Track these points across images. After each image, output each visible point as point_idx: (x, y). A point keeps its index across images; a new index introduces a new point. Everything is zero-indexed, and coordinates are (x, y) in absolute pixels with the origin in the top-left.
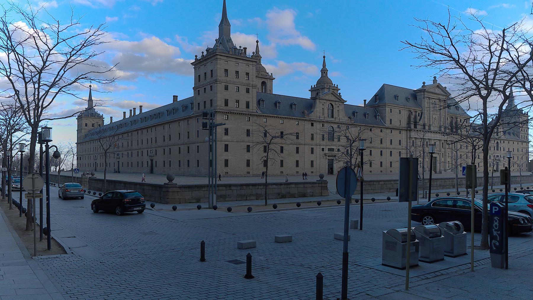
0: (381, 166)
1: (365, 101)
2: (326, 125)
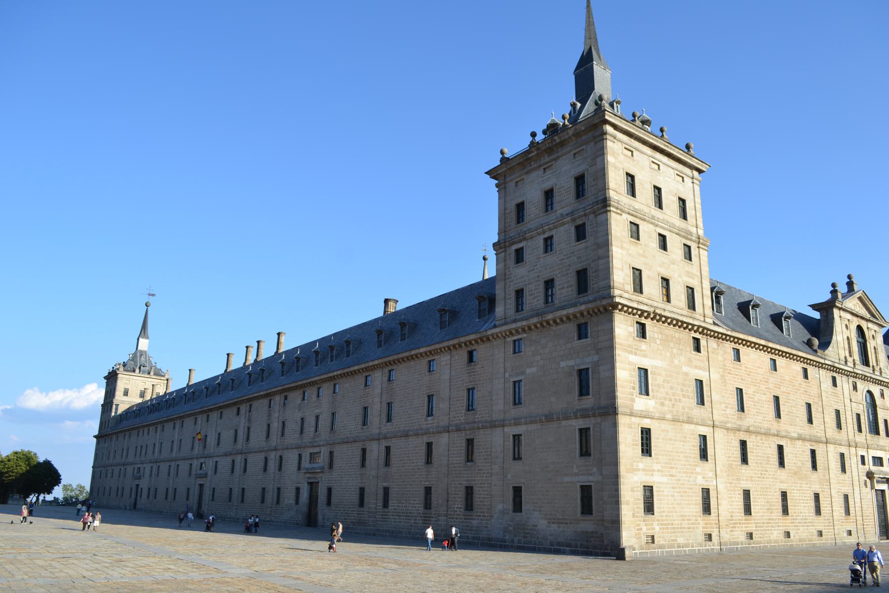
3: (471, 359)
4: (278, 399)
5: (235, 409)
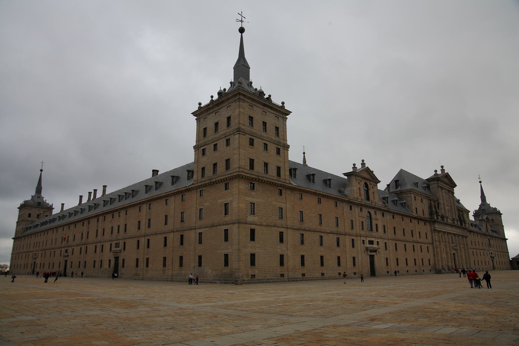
0: (415, 265)
2: (364, 209)
4: (101, 218)
5: (82, 223)
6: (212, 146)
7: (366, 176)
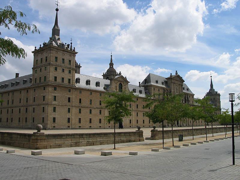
1: (140, 83)
3: (27, 92)
6: (40, 69)
7: (121, 79)
